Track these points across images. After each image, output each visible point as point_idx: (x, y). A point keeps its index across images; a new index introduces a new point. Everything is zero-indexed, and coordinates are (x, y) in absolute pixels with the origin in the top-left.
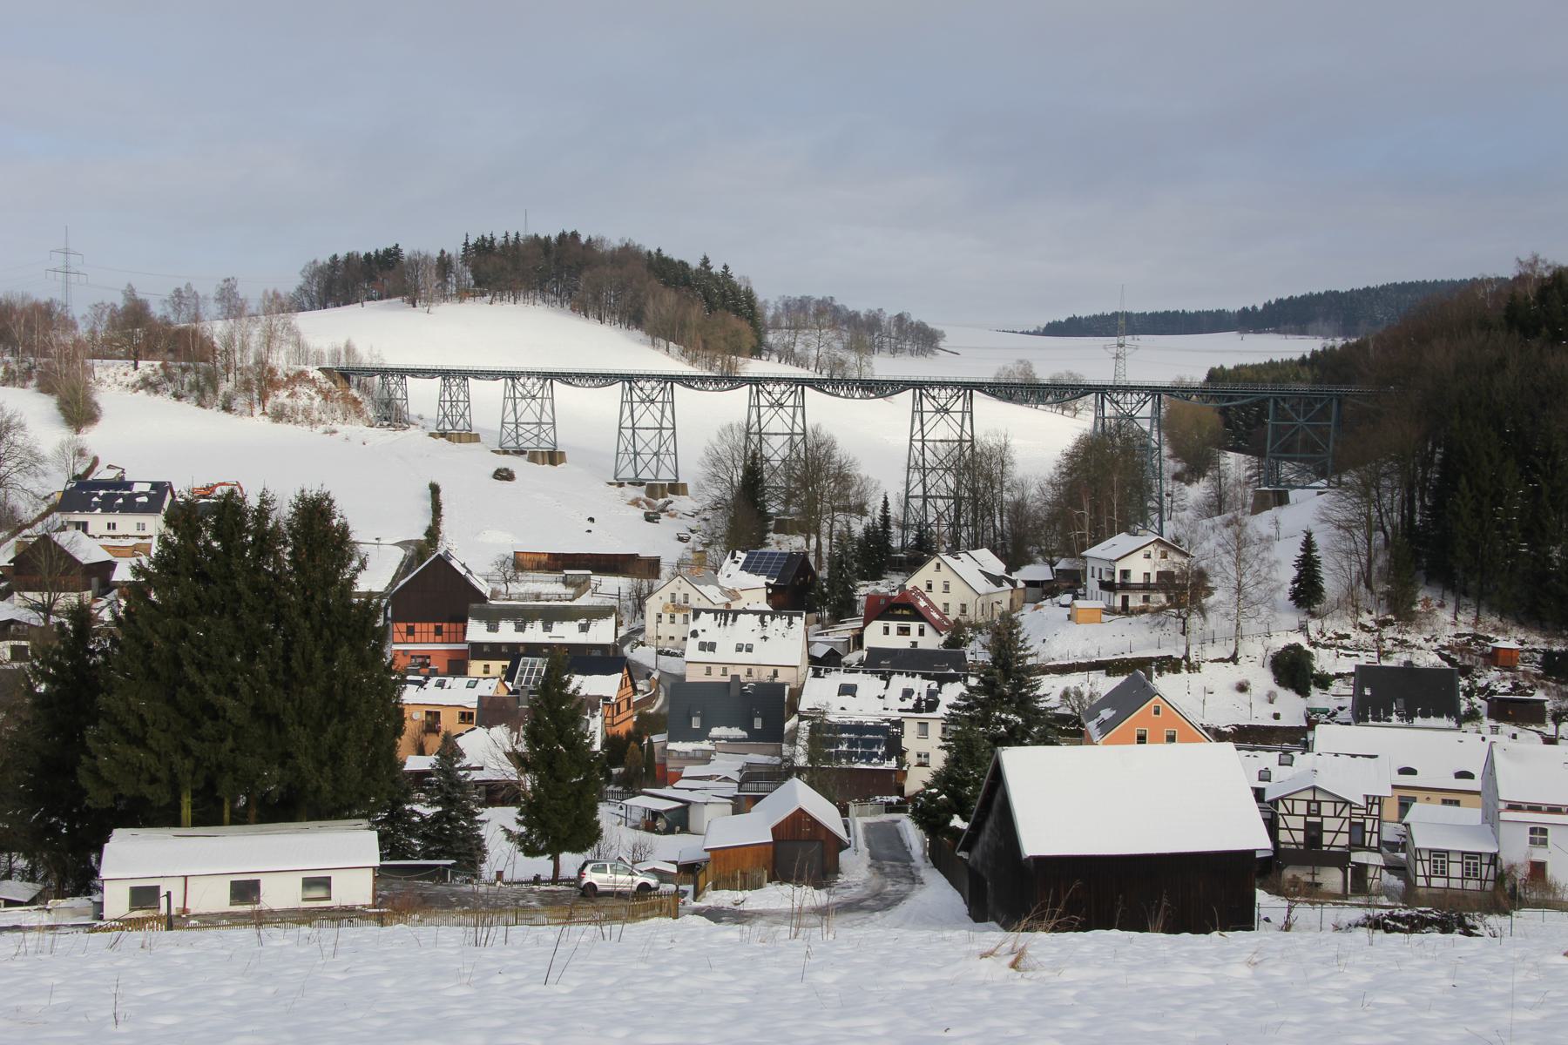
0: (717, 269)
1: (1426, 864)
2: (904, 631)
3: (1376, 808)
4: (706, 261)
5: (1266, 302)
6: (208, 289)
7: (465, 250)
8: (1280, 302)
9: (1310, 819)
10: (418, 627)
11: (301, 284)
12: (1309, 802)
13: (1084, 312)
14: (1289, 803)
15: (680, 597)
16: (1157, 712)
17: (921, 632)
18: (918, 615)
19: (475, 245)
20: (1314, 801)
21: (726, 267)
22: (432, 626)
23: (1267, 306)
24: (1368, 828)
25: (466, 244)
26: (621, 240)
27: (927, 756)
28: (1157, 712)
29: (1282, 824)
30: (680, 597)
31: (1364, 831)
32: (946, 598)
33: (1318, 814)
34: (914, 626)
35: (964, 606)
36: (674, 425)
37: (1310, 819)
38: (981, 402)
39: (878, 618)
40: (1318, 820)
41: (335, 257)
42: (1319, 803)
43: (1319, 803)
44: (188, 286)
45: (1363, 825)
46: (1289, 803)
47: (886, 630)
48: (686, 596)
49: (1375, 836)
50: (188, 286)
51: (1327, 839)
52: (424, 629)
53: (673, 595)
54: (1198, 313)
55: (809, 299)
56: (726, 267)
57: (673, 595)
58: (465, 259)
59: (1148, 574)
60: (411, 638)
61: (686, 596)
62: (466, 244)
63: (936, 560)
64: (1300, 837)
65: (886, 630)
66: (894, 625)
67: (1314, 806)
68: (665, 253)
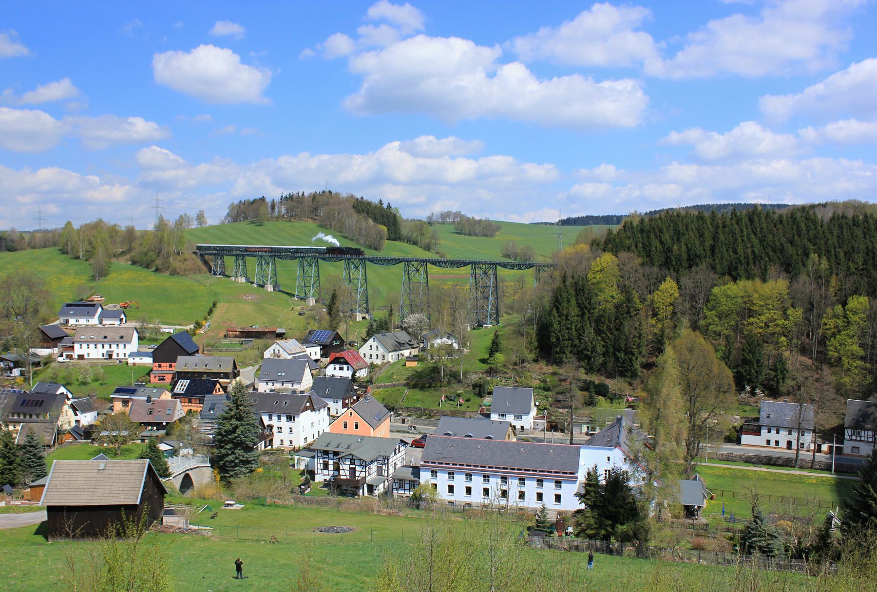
0: (385, 206)
1: (397, 484)
2: (341, 369)
3: (386, 460)
4: (381, 201)
6: (193, 214)
7: (281, 199)
9: (351, 466)
10: (163, 364)
11: (139, 227)
12: (351, 459)
13: (574, 215)
14: (344, 460)
15: (276, 351)
16: (351, 415)
18: (346, 363)
19: (286, 197)
20: (353, 459)
21: (389, 204)
24: (384, 468)
25: (282, 197)
26: (347, 193)
27: (281, 428)
28: (351, 415)
29: (341, 468)
30: (276, 351)
31: (382, 470)
32: (377, 352)
33: (354, 464)
34: (345, 367)
36: (318, 274)
37: (351, 466)
38: (429, 265)
40: (354, 466)
41: (241, 201)
42: (354, 460)
43: (354, 460)
44: (185, 214)
45: (382, 467)
46: (344, 460)
47: (335, 369)
48: (279, 350)
49: (386, 472)
50: (185, 214)
51: (357, 474)
53: (274, 350)
54: (621, 216)
55: (451, 212)
56: (389, 204)
57: (274, 350)
58: (281, 203)
60: (160, 369)
61: (279, 350)
62: (282, 197)
63: (374, 337)
64: (348, 473)
65: (335, 369)
66: (337, 366)
67: (353, 461)
68: (365, 198)
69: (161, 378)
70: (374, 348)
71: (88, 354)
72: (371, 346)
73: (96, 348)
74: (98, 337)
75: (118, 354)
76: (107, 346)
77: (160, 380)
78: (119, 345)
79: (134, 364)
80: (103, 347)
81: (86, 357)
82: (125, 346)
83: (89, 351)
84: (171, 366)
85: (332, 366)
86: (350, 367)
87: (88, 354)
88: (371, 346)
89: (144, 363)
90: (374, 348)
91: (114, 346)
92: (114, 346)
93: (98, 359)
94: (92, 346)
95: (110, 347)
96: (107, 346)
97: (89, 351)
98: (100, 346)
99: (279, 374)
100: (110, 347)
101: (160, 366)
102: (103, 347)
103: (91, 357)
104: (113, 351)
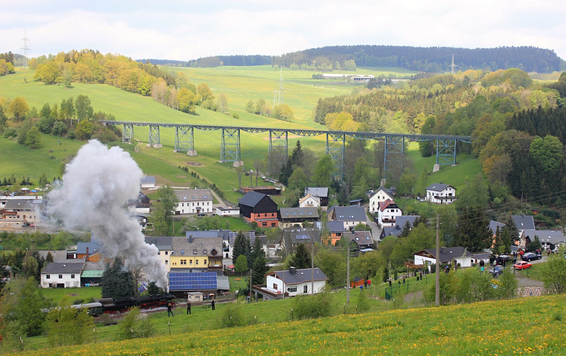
2: (393, 211)
5: (283, 54)
8: (288, 54)
15: (310, 203)
17: (397, 211)
22: (264, 214)
23: (283, 56)
30: (310, 203)
34: (395, 210)
35: (374, 202)
39: (386, 208)
47: (388, 211)
48: (312, 202)
52: (269, 215)
53: (308, 202)
54: (250, 56)
57: (308, 202)
59: (447, 194)
61: (312, 202)
65: (388, 211)
66: (390, 210)
69: (264, 223)
70: (381, 198)
71: (183, 210)
72: (379, 197)
73: (188, 205)
74: (188, 197)
75: (203, 209)
76: (196, 204)
77: (263, 225)
78: (199, 203)
79: (225, 216)
80: (193, 205)
81: (181, 212)
82: (208, 203)
83: (183, 208)
84: (266, 215)
85: (386, 210)
86: (398, 209)
87: (183, 210)
88: (379, 197)
89: (231, 215)
90: (381, 198)
91: (201, 203)
92: (201, 203)
93: (190, 214)
94: (186, 204)
95: (198, 205)
96: (196, 204)
97: (183, 208)
98: (191, 204)
99: (341, 217)
100: (198, 205)
101: (259, 216)
102: (193, 205)
103: (185, 212)
104: (200, 208)
